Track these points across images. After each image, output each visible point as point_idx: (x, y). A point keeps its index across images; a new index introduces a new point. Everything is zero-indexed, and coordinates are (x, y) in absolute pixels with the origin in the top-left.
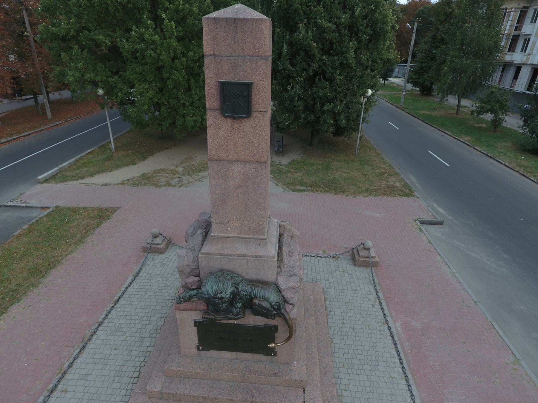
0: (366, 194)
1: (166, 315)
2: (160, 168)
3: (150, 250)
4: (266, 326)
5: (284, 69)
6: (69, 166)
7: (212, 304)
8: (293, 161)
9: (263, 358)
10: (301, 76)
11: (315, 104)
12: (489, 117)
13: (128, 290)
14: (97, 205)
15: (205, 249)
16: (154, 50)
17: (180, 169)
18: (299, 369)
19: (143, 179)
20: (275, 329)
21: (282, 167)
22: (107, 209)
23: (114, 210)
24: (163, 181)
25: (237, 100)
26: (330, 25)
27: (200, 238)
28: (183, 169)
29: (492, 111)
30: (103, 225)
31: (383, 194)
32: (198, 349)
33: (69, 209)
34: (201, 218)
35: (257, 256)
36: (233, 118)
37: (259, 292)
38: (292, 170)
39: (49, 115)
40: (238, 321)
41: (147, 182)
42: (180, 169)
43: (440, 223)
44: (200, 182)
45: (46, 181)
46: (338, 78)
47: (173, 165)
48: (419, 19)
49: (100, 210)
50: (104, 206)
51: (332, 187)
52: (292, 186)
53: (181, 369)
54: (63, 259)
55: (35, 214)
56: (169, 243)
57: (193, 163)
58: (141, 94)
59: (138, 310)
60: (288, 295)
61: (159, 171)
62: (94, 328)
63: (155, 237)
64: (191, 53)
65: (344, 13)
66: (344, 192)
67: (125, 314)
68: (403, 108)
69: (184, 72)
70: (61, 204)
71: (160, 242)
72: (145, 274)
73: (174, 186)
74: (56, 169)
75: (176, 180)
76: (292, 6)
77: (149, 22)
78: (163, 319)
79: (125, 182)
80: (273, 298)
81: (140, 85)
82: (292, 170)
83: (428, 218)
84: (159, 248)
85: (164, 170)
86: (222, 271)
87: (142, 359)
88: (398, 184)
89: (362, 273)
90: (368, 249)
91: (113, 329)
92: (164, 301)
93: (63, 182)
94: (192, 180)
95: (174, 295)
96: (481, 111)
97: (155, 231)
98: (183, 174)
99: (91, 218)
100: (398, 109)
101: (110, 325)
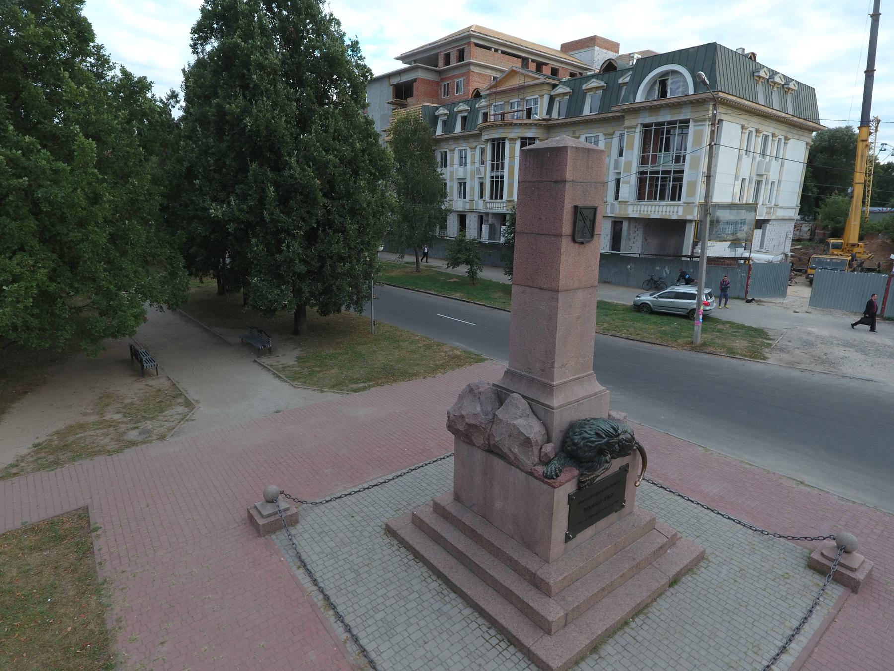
0: (442, 371)
1: (426, 575)
2: (60, 426)
5: (273, 220)
8: (298, 359)
9: (614, 516)
11: (322, 267)
12: (463, 270)
13: (321, 584)
14: (18, 524)
15: (556, 401)
19: (52, 454)
20: (624, 470)
22: (52, 523)
23: (83, 515)
24: (105, 441)
27: (524, 401)
28: (119, 416)
29: (468, 262)
30: (97, 544)
32: (567, 539)
34: (482, 390)
35: (596, 394)
36: (582, 243)
38: (317, 369)
41: (69, 454)
42: (113, 415)
44: (190, 423)
46: (352, 227)
47: (85, 414)
49: (32, 530)
50: (35, 519)
53: (566, 574)
54: (103, 622)
57: (127, 401)
59: (380, 593)
61: (71, 430)
62: (351, 648)
66: (415, 375)
67: (369, 607)
71: (287, 506)
72: (315, 557)
73: (151, 442)
76: (275, 131)
78: (429, 580)
79: (14, 470)
81: (10, 258)
82: (317, 369)
84: (291, 516)
85: (82, 427)
87: (474, 626)
88: (458, 353)
91: (383, 630)
92: (396, 565)
94: (167, 425)
95: (398, 553)
96: (455, 263)
97: (273, 488)
99: (37, 548)
101: (369, 630)
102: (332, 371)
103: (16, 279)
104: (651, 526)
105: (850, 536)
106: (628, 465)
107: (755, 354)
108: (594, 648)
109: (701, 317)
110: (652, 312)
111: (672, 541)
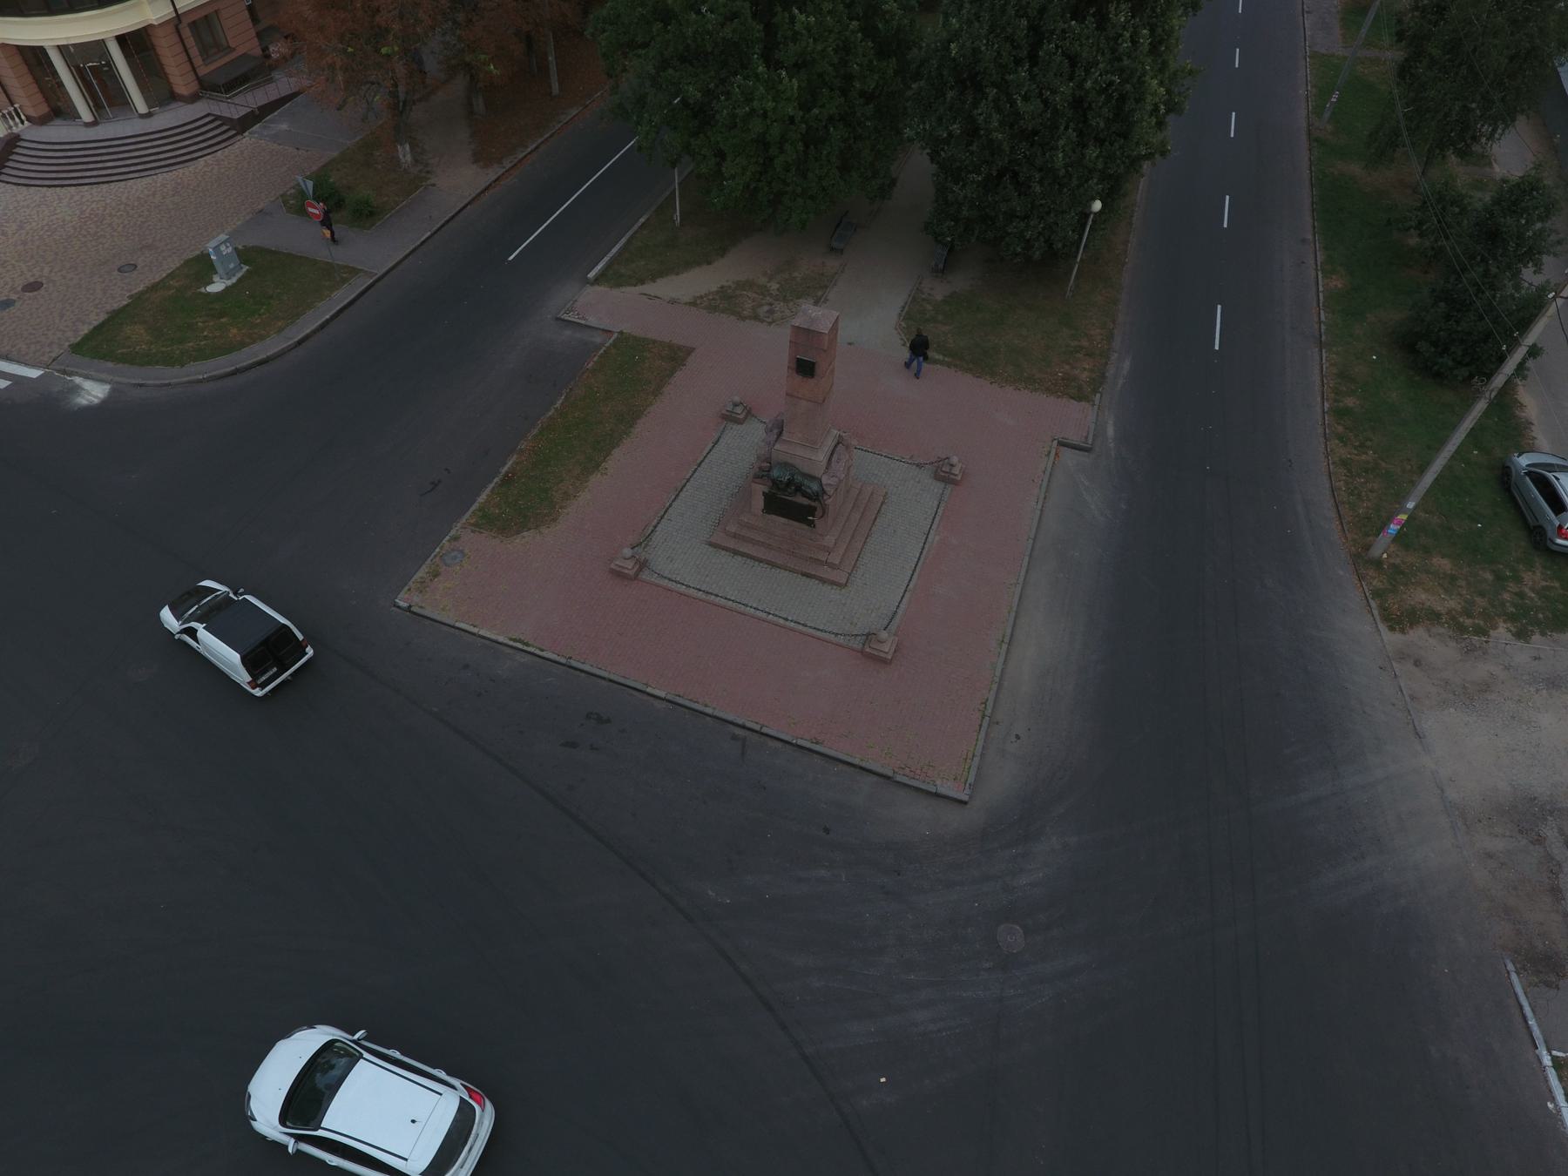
3: (729, 418)
4: (810, 506)
6: (620, 253)
7: (775, 483)
15: (777, 446)
17: (774, 286)
18: (829, 540)
20: (815, 509)
21: (929, 307)
23: (690, 351)
30: (678, 373)
31: (1048, 390)
37: (806, 482)
40: (790, 499)
55: (598, 340)
56: (749, 413)
58: (733, 177)
63: (736, 405)
64: (816, 111)
68: (1316, 140)
70: (627, 328)
74: (606, 259)
75: (766, 308)
80: (815, 487)
83: (1075, 439)
85: (749, 285)
86: (786, 464)
89: (938, 487)
93: (619, 285)
94: (787, 313)
97: (737, 399)
100: (1304, 137)
103: (733, 177)
105: (884, 635)
108: (736, 553)
109: (1393, 528)
111: (833, 566)
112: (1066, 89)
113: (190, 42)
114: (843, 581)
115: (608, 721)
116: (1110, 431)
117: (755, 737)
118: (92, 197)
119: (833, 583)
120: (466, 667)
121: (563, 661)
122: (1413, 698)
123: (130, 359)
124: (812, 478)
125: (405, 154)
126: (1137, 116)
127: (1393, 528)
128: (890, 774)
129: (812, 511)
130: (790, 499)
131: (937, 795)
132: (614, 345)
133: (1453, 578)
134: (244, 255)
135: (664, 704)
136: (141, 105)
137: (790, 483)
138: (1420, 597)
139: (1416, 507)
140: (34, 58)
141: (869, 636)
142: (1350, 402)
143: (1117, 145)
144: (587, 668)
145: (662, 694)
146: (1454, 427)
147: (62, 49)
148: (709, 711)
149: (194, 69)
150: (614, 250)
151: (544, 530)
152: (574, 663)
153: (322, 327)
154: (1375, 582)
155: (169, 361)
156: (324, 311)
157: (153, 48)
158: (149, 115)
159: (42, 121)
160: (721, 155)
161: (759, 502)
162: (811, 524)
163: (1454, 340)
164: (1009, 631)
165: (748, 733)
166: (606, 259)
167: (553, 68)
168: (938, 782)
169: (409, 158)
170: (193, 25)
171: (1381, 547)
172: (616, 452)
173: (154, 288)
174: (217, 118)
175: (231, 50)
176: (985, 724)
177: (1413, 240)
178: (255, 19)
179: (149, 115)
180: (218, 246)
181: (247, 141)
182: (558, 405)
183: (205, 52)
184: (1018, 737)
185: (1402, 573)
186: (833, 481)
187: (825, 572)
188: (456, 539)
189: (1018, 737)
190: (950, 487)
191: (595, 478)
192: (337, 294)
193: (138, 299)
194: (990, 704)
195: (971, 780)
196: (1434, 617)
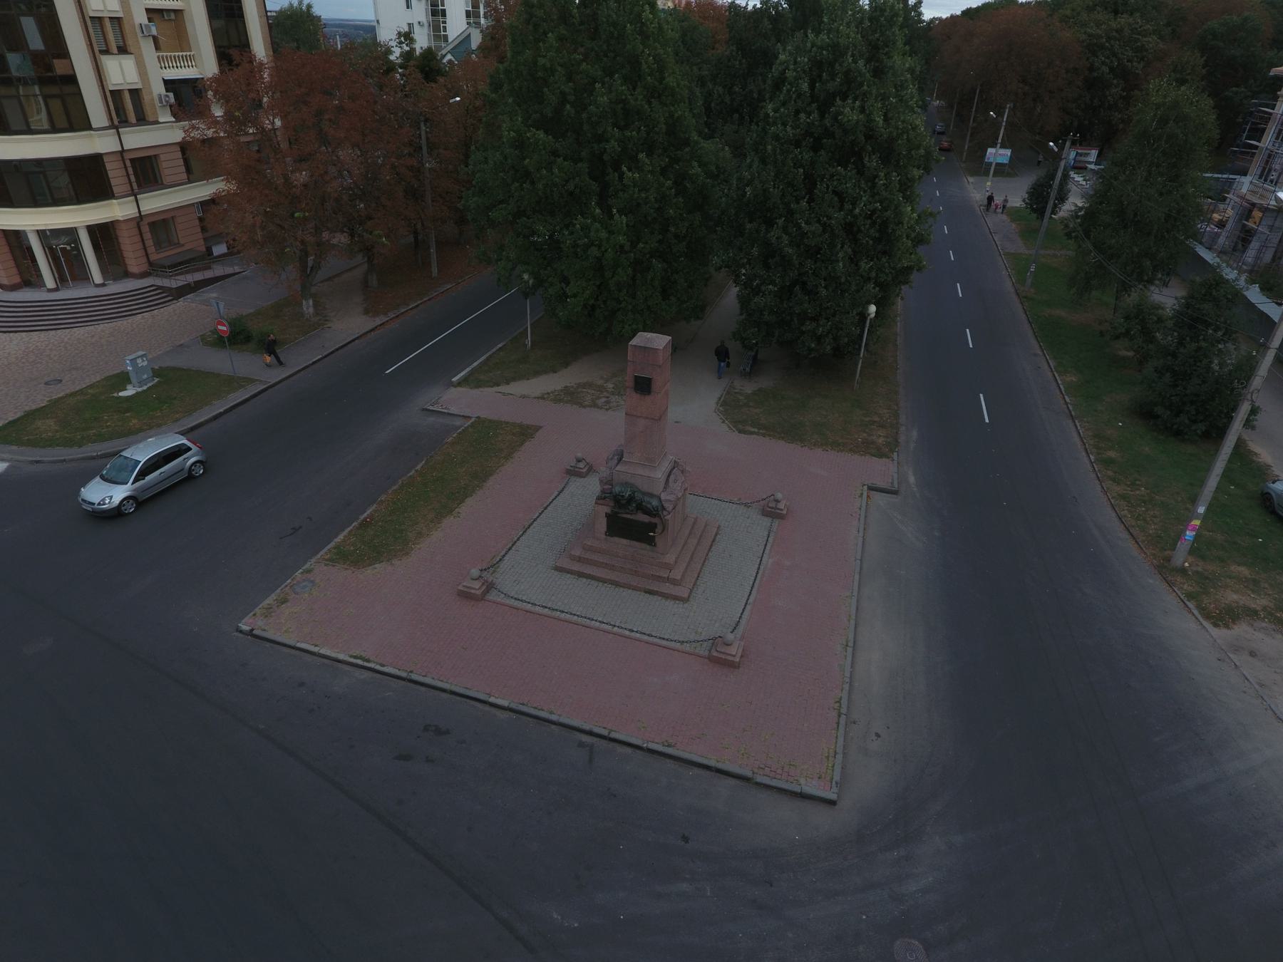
3: (573, 472)
10: (775, 285)
15: (618, 468)
16: (600, 247)
17: (610, 386)
18: (670, 558)
20: (655, 525)
22: (528, 427)
23: (538, 428)
25: (643, 386)
26: (816, 227)
31: (851, 450)
33: (490, 421)
37: (647, 499)
39: (435, 271)
40: (632, 519)
43: (895, 493)
45: (459, 384)
48: (1075, 135)
49: (521, 426)
51: (792, 433)
52: (740, 425)
55: (458, 422)
56: (591, 469)
58: (575, 296)
60: (666, 505)
61: (584, 385)
63: (579, 461)
64: (641, 245)
65: (841, 209)
69: (630, 271)
74: (468, 369)
77: (598, 211)
80: (655, 503)
85: (589, 385)
88: (881, 440)
90: (777, 501)
93: (478, 387)
97: (579, 455)
98: (613, 394)
102: (757, 411)
103: (575, 296)
104: (669, 567)
105: (730, 637)
106: (655, 525)
107: (1225, 617)
108: (581, 575)
109: (1190, 534)
110: (1273, 512)
112: (839, 215)
113: (147, 236)
114: (686, 595)
115: (447, 732)
116: (912, 479)
117: (604, 742)
118: (37, 339)
119: (676, 598)
120: (302, 684)
121: (404, 675)
122: (1262, 685)
123: (33, 444)
124: (652, 495)
125: (308, 307)
126: (898, 233)
127: (1190, 534)
128: (749, 774)
129: (653, 527)
130: (632, 519)
131: (803, 796)
132: (472, 425)
133: (1255, 582)
134: (156, 373)
135: (506, 715)
136: (97, 276)
137: (631, 499)
138: (1231, 597)
139: (1208, 509)
140: (15, 239)
141: (715, 641)
142: (1112, 454)
143: (884, 260)
144: (428, 680)
145: (505, 703)
146: (1208, 470)
147: (41, 234)
148: (554, 718)
149: (147, 255)
150: (475, 364)
151: (395, 562)
152: (414, 677)
153: (216, 418)
154: (1185, 587)
155: (69, 443)
156: (219, 407)
157: (119, 243)
158: (103, 285)
159: (13, 288)
160: (566, 280)
161: (602, 525)
162: (651, 542)
163: (1184, 402)
164: (851, 637)
165: (595, 739)
166: (468, 369)
167: (434, 257)
168: (802, 781)
169: (311, 310)
170: (153, 225)
171: (1181, 557)
172: (469, 501)
173: (73, 394)
174: (159, 288)
175: (179, 245)
176: (843, 721)
177: (1124, 350)
178: (204, 229)
179: (103, 285)
180: (137, 361)
181: (181, 303)
182: (419, 467)
183: (158, 245)
184: (878, 735)
185: (1207, 578)
186: (672, 497)
187: (667, 588)
188: (309, 571)
189: (878, 735)
190: (777, 522)
191: (448, 521)
192: (232, 396)
193: (55, 403)
194: (844, 702)
195: (837, 778)
196: (1252, 614)
